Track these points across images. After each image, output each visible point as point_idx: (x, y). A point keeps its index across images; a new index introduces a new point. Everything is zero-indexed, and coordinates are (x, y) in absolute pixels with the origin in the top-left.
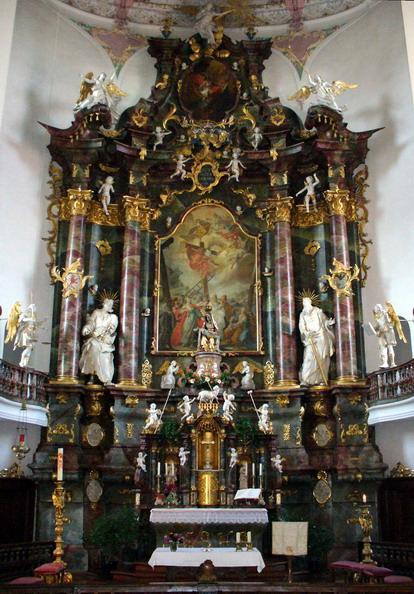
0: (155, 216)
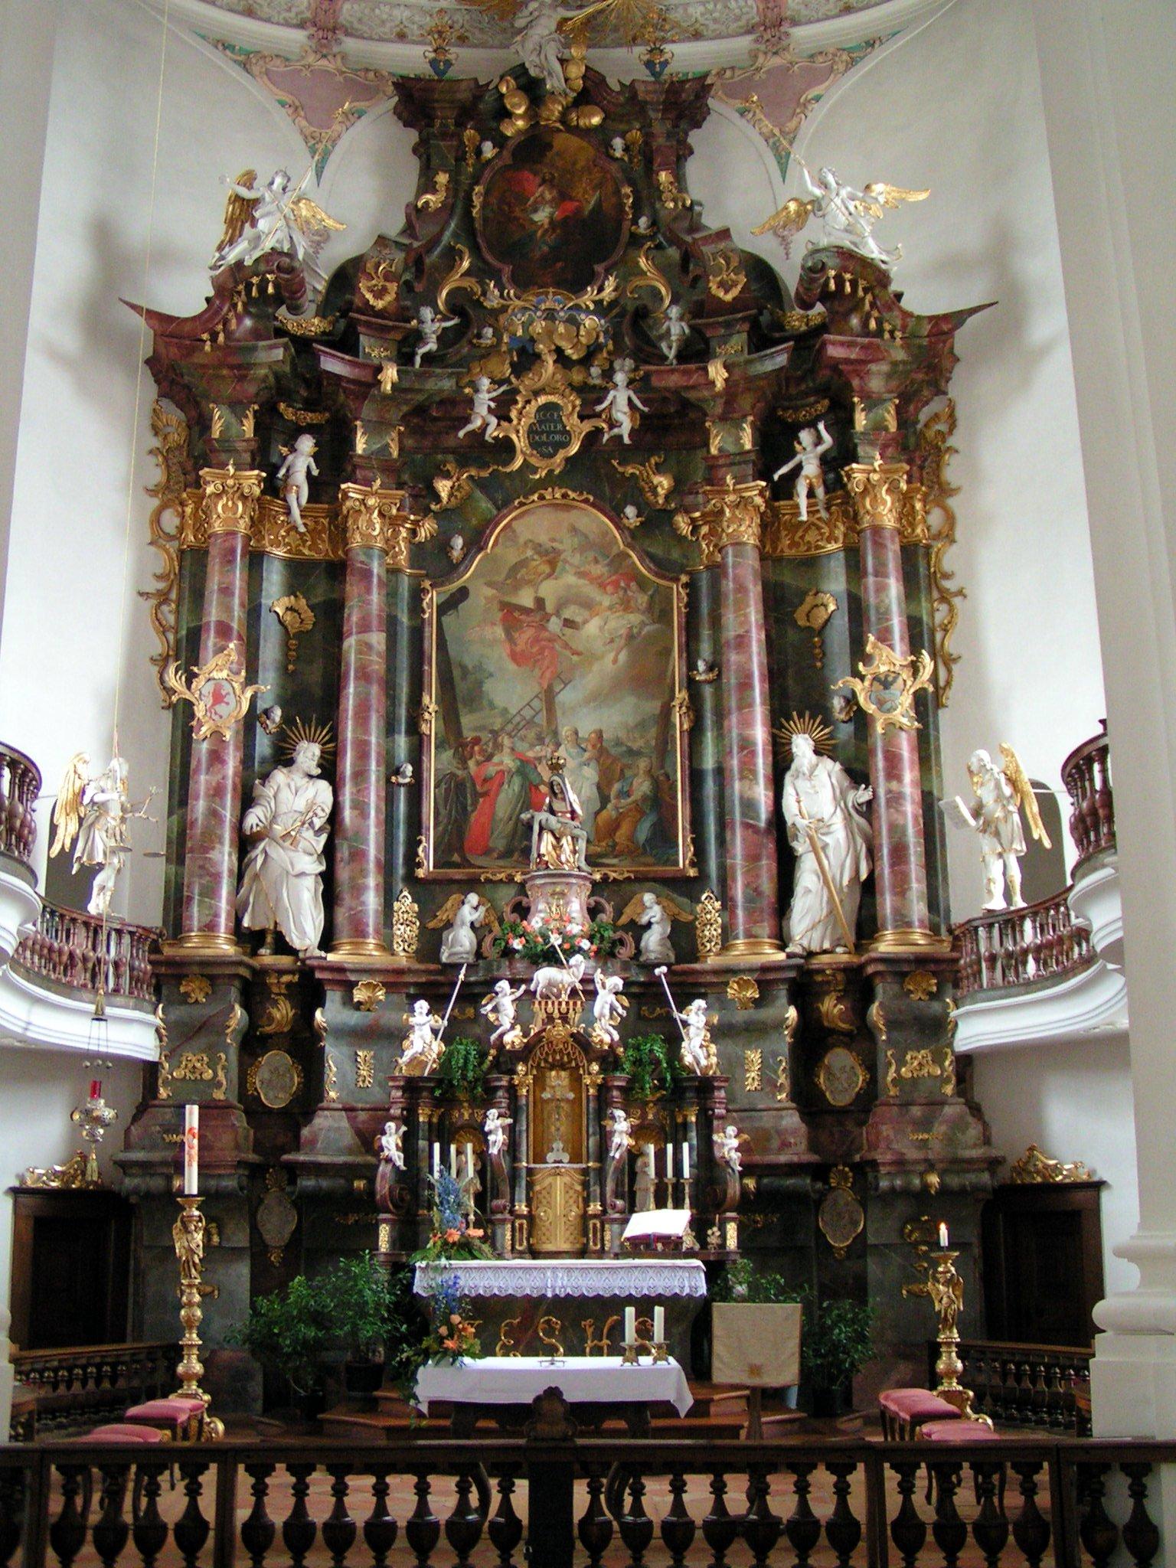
0: (423, 534)
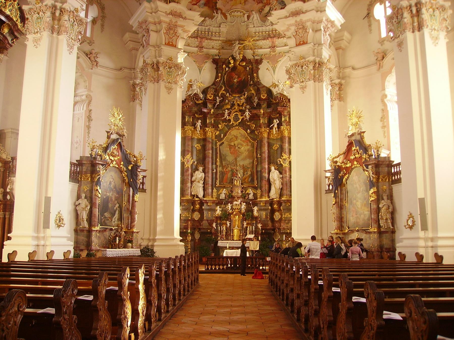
0: (217, 134)
